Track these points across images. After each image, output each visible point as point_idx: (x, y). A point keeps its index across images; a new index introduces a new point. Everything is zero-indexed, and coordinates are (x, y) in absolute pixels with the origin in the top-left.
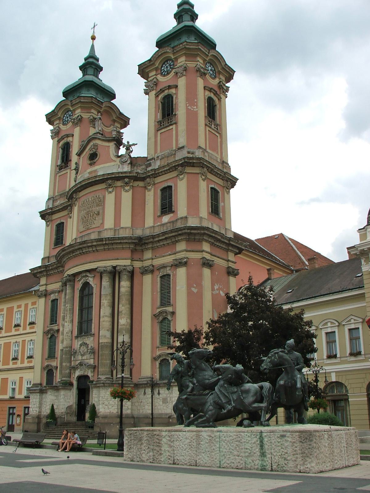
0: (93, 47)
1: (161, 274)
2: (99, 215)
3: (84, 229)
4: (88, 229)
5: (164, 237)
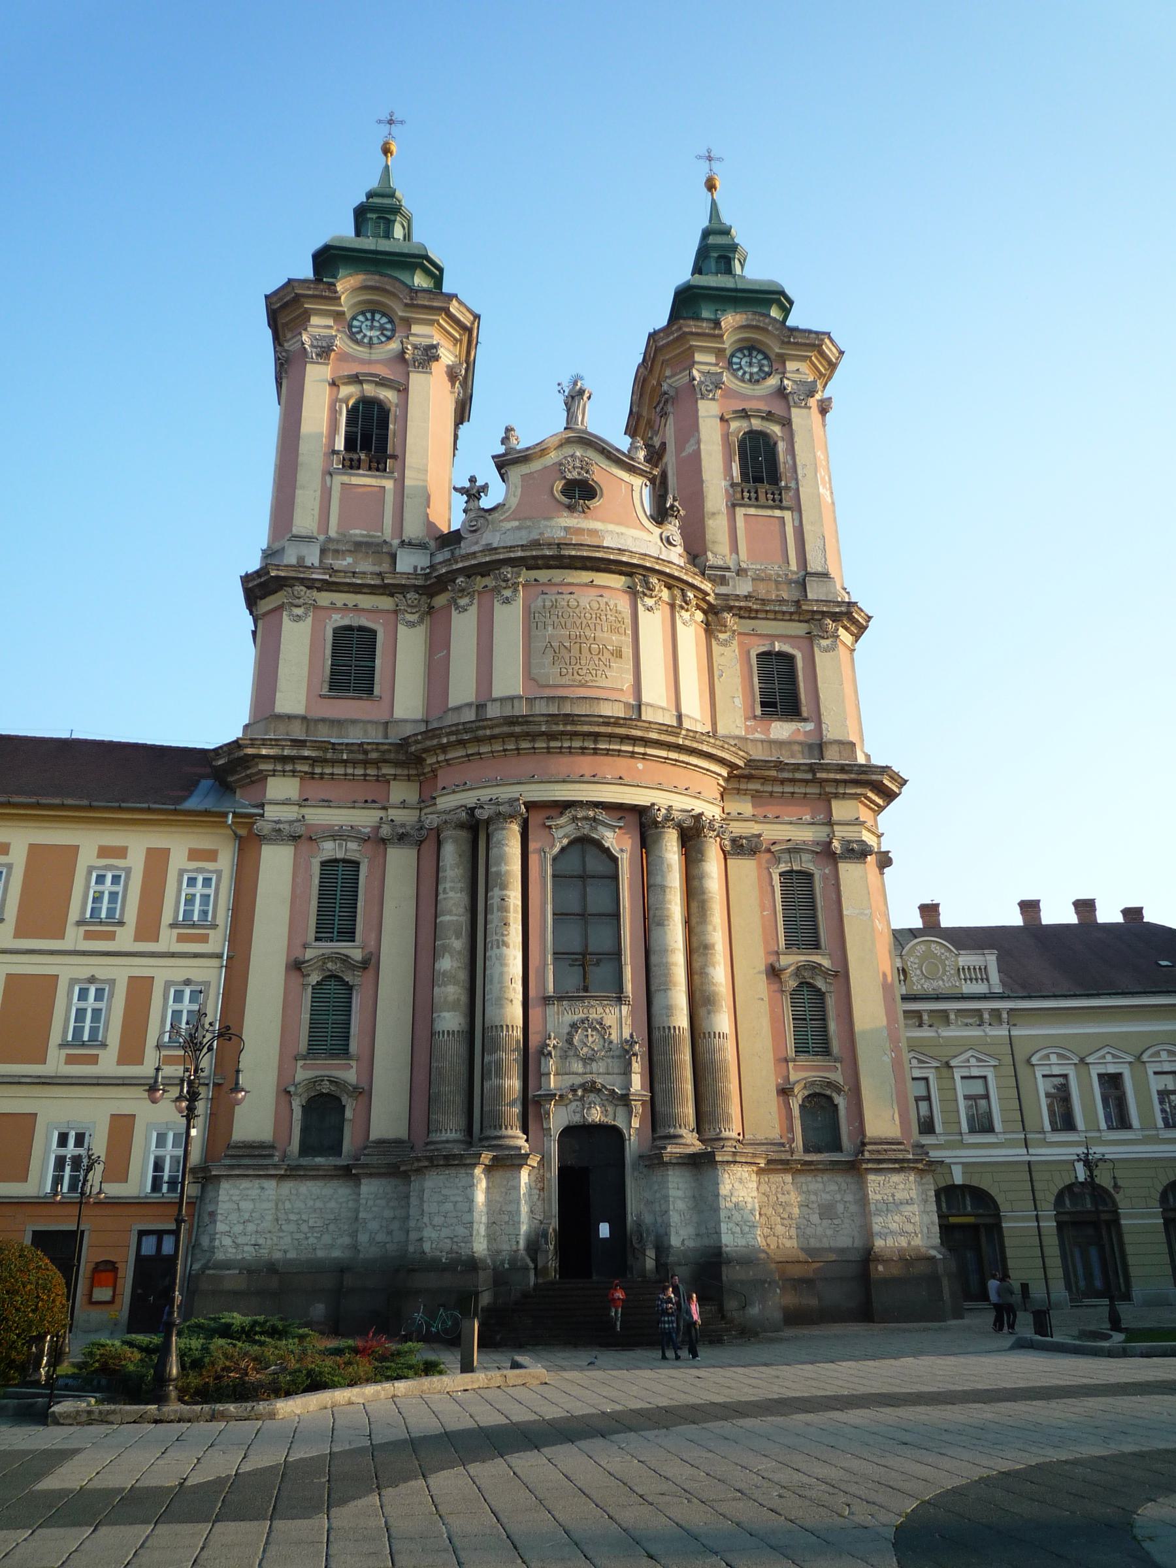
1: (781, 865)
2: (621, 657)
3: (564, 681)
5: (809, 776)
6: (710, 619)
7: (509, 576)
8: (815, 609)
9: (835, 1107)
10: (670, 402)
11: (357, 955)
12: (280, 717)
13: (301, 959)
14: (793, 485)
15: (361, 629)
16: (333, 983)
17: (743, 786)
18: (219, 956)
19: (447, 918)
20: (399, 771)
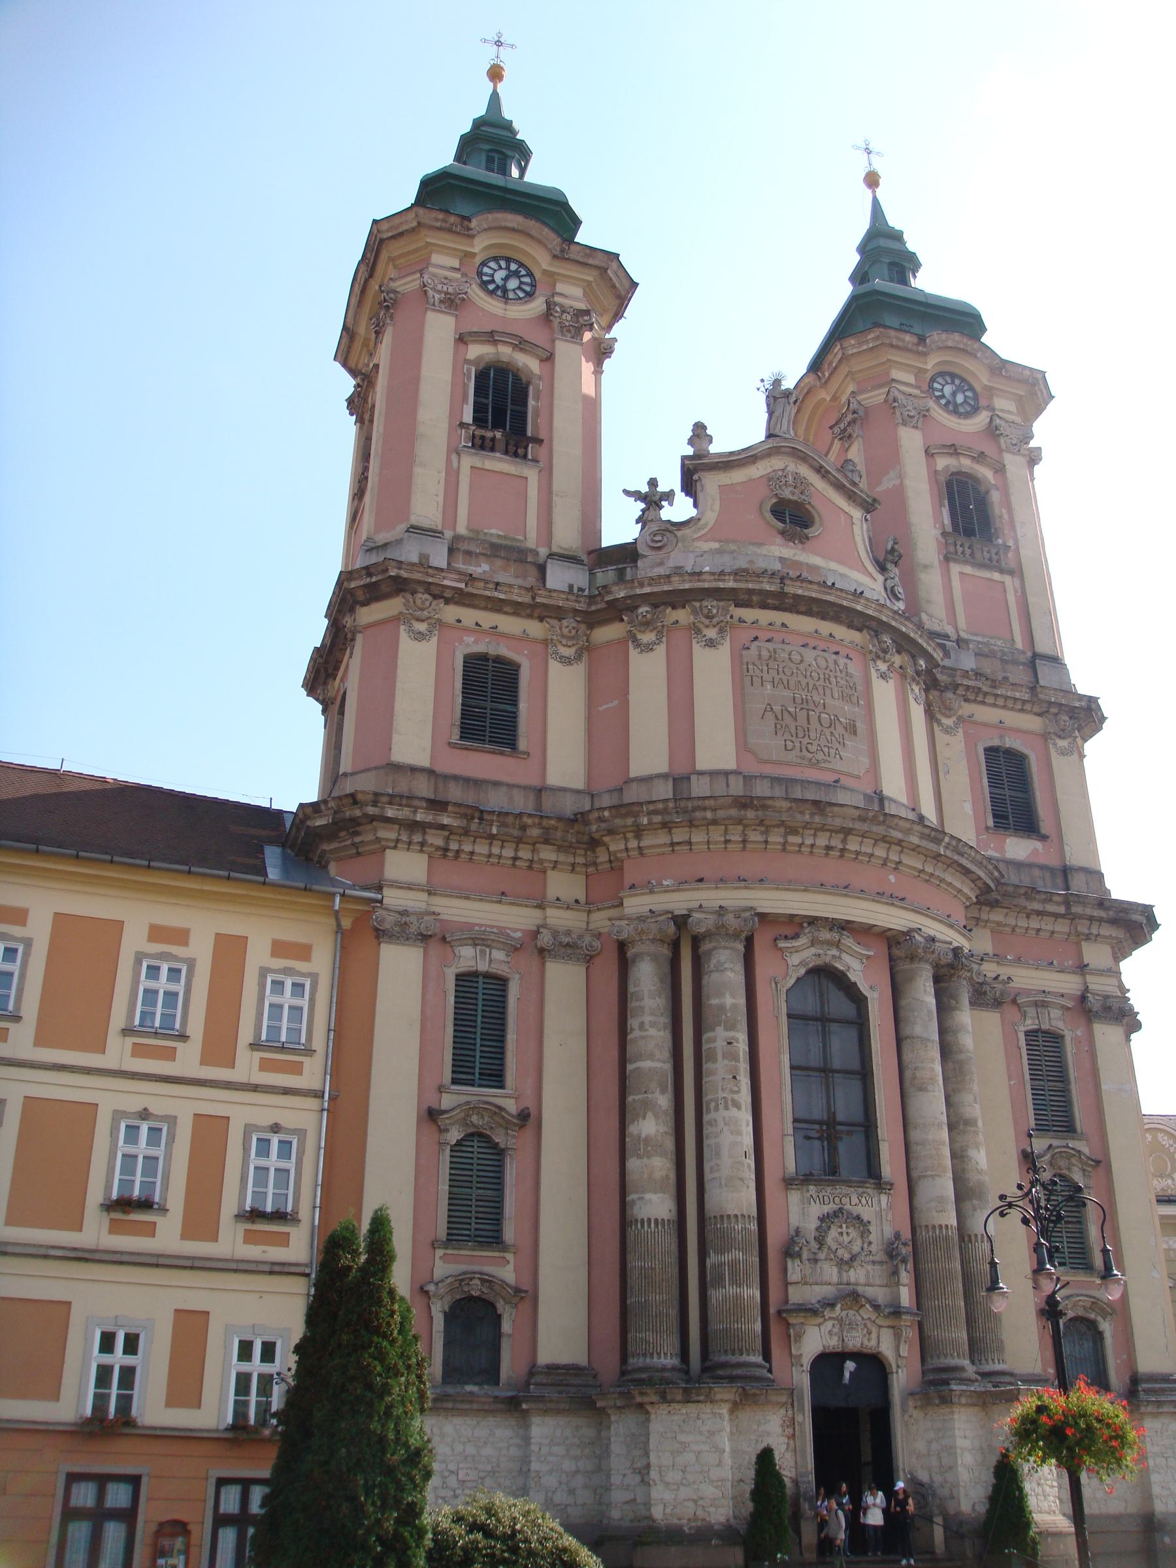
0: (495, 99)
1: (1029, 1022)
2: (855, 733)
3: (792, 757)
4: (815, 764)
5: (1061, 910)
6: (931, 698)
7: (715, 611)
8: (1053, 700)
9: (1100, 1335)
10: (859, 422)
11: (511, 1106)
12: (397, 768)
13: (435, 1106)
14: (1011, 543)
15: (498, 660)
16: (476, 1144)
17: (984, 916)
18: (319, 1095)
19: (647, 1064)
20: (562, 858)
